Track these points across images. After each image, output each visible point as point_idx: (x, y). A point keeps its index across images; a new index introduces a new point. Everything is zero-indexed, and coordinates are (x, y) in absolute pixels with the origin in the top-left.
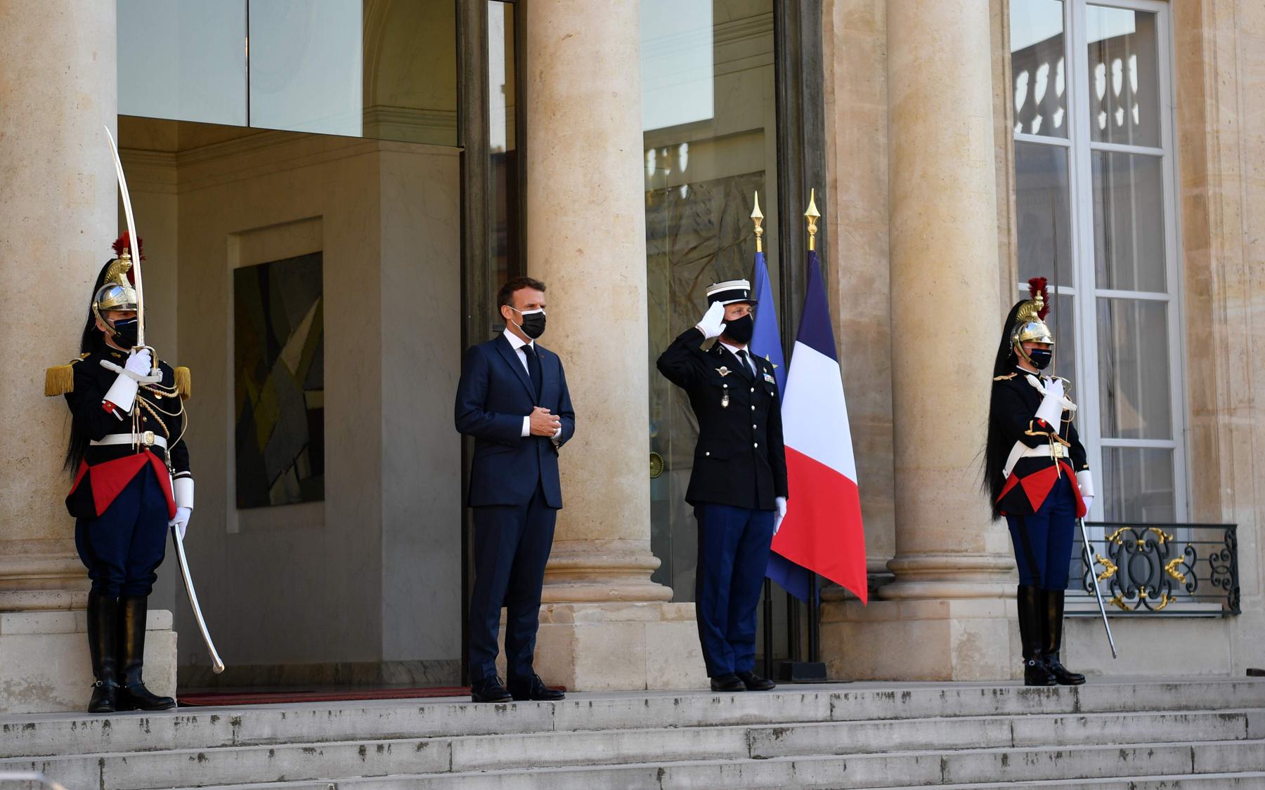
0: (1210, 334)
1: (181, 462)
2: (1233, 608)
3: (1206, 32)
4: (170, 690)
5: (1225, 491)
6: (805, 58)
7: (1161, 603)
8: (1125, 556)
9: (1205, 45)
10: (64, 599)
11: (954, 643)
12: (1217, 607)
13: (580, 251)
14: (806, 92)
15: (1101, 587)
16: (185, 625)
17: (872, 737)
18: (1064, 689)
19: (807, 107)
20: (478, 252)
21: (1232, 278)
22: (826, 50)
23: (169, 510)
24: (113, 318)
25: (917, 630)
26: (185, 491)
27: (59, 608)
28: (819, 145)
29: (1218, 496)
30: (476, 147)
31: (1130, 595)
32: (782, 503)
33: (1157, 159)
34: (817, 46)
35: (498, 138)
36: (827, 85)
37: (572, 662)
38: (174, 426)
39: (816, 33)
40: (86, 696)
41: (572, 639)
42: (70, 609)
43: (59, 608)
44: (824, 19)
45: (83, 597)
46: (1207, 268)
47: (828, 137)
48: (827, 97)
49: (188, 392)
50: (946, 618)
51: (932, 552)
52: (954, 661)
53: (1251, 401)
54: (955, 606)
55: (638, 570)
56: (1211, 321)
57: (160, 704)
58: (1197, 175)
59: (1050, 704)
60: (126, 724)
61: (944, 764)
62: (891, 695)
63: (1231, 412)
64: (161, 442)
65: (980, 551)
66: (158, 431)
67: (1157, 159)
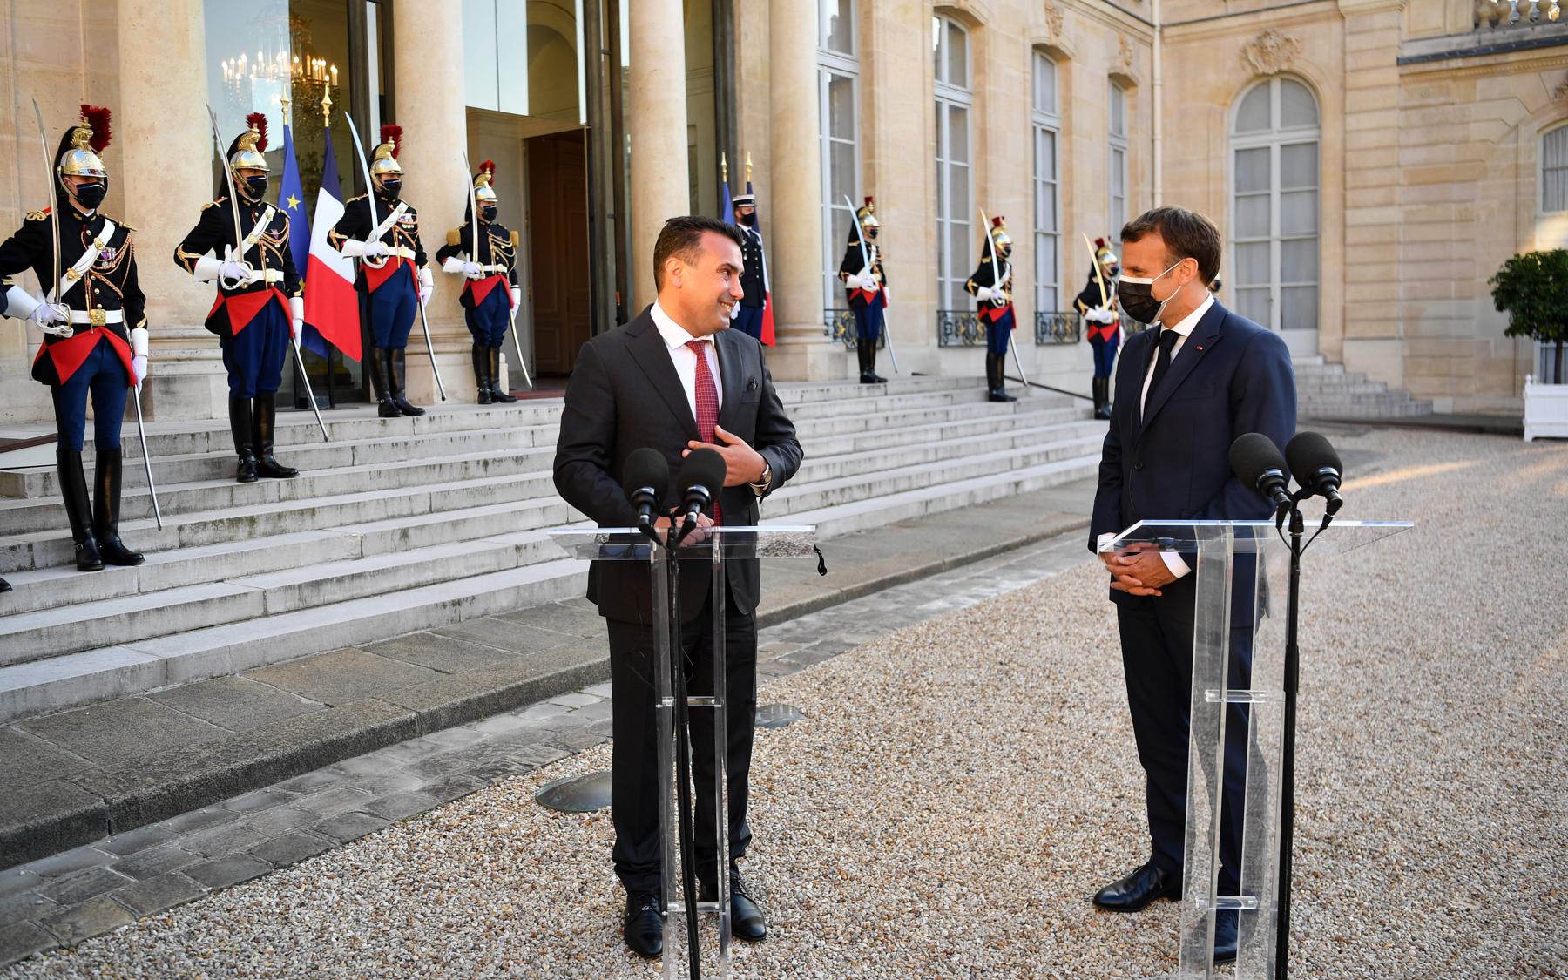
1: (514, 281)
3: (876, 89)
6: (729, 90)
8: (847, 324)
10: (458, 348)
13: (662, 178)
14: (730, 106)
16: (513, 360)
18: (882, 385)
19: (730, 114)
20: (599, 178)
22: (737, 86)
23: (510, 305)
24: (482, 205)
25: (790, 359)
26: (516, 295)
27: (456, 352)
28: (735, 132)
32: (765, 302)
33: (851, 147)
34: (733, 84)
36: (738, 104)
38: (511, 260)
39: (733, 74)
42: (461, 352)
43: (456, 352)
44: (737, 72)
47: (738, 128)
48: (738, 111)
49: (518, 244)
50: (804, 353)
51: (795, 323)
52: (809, 372)
54: (810, 348)
58: (870, 153)
59: (877, 392)
60: (498, 411)
61: (866, 423)
62: (823, 390)
64: (505, 269)
65: (815, 323)
66: (505, 264)
67: (851, 147)
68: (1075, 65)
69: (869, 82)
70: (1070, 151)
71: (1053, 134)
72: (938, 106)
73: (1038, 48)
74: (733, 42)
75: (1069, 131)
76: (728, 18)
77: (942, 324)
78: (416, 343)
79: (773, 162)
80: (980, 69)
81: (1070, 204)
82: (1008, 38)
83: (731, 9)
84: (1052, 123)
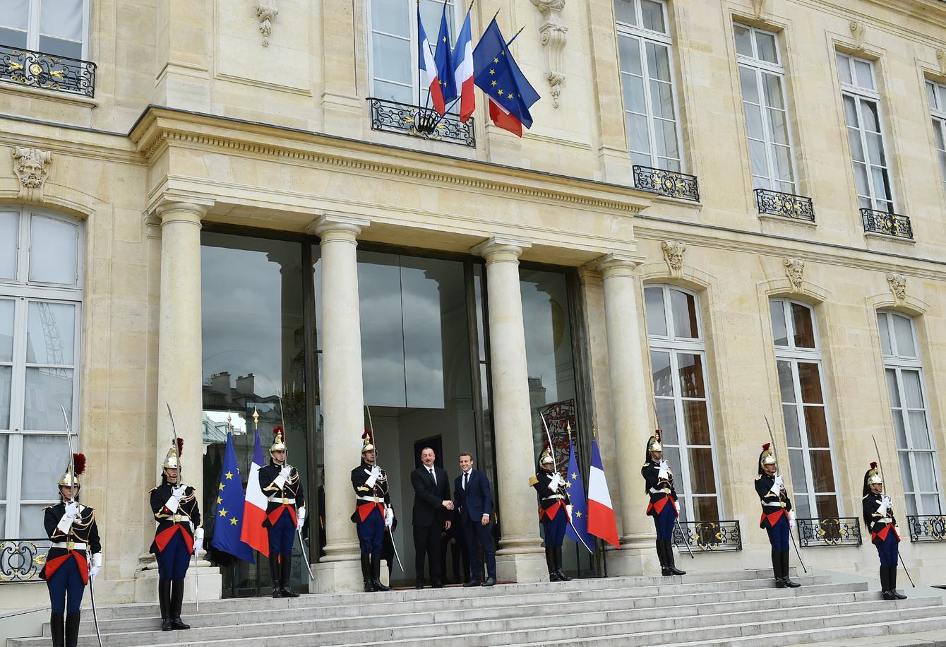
0: (726, 458)
2: (740, 548)
3: (717, 360)
4: (387, 585)
5: (735, 510)
7: (715, 547)
9: (717, 364)
11: (643, 563)
12: (735, 548)
15: (695, 543)
17: (609, 594)
20: (481, 443)
21: (732, 439)
25: (630, 559)
27: (351, 560)
28: (590, 403)
29: (732, 512)
30: (479, 410)
31: (704, 545)
35: (485, 406)
37: (516, 572)
40: (362, 587)
41: (515, 566)
43: (351, 560)
45: (359, 556)
46: (723, 436)
53: (741, 479)
55: (535, 544)
56: (726, 454)
57: (383, 589)
58: (718, 407)
63: (735, 483)
68: (927, 318)
69: (712, 356)
70: (933, 385)
71: (918, 371)
72: (783, 368)
73: (883, 312)
74: (586, 344)
75: (929, 371)
76: (581, 328)
77: (801, 530)
78: (329, 555)
79: (613, 420)
80: (823, 334)
81: (939, 426)
82: (850, 308)
83: (583, 323)
84: (912, 364)
